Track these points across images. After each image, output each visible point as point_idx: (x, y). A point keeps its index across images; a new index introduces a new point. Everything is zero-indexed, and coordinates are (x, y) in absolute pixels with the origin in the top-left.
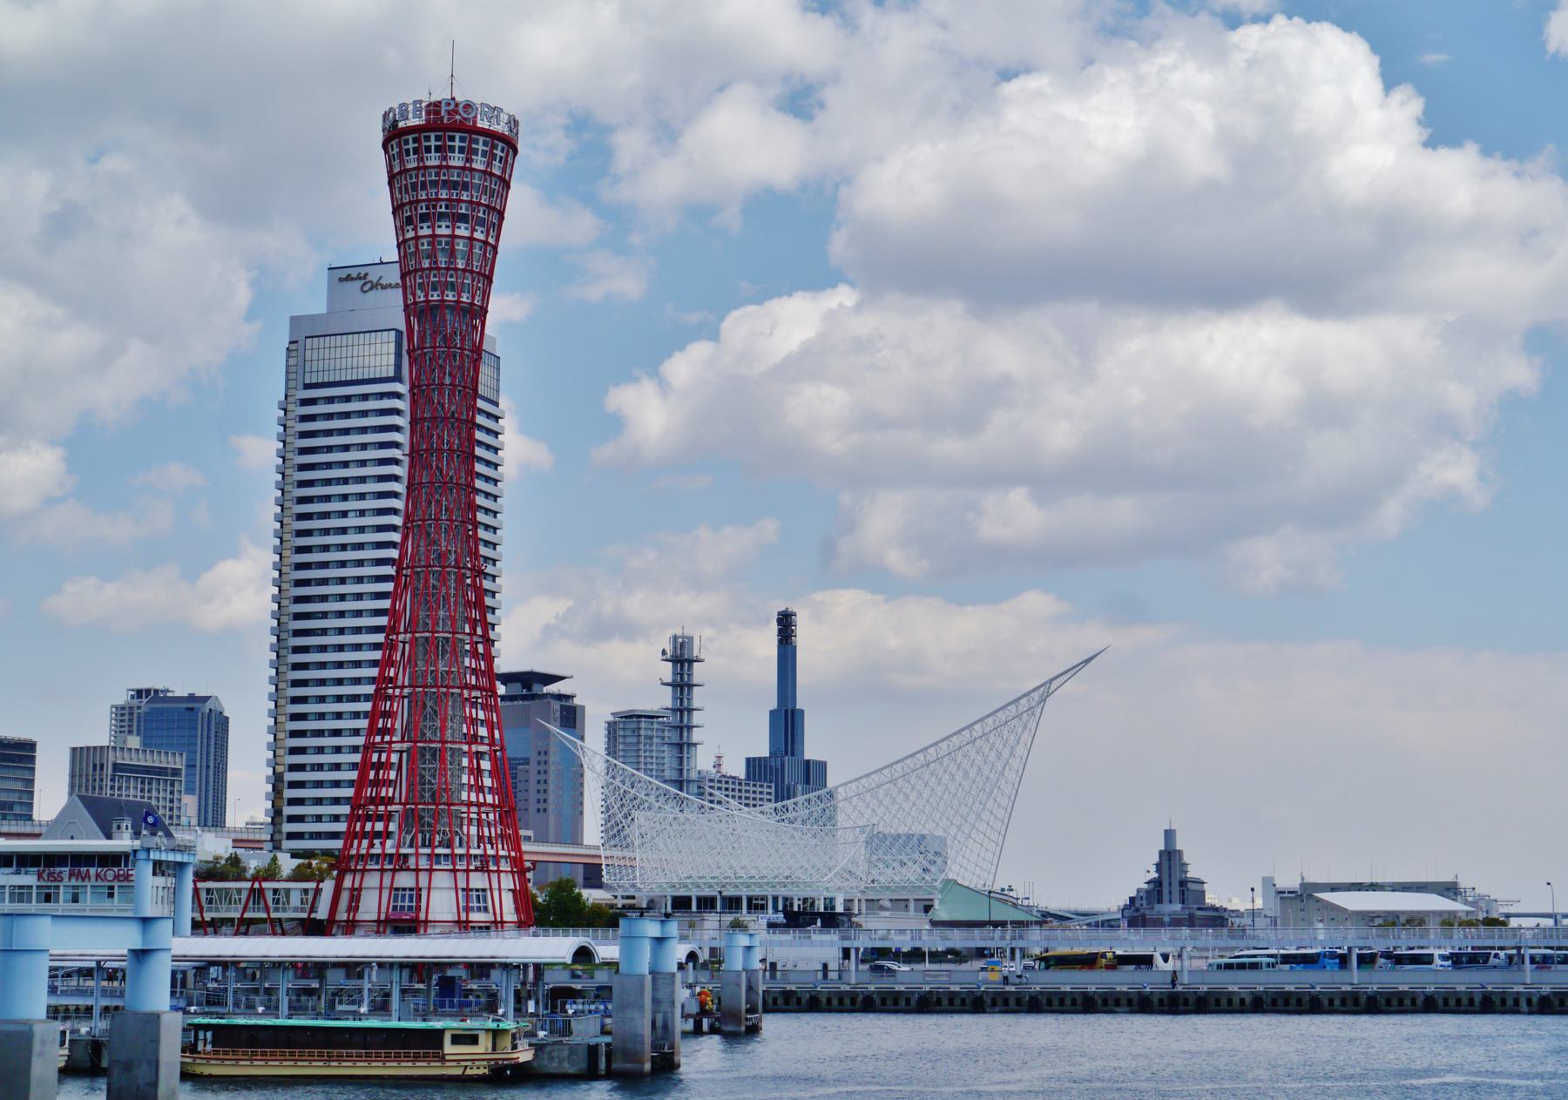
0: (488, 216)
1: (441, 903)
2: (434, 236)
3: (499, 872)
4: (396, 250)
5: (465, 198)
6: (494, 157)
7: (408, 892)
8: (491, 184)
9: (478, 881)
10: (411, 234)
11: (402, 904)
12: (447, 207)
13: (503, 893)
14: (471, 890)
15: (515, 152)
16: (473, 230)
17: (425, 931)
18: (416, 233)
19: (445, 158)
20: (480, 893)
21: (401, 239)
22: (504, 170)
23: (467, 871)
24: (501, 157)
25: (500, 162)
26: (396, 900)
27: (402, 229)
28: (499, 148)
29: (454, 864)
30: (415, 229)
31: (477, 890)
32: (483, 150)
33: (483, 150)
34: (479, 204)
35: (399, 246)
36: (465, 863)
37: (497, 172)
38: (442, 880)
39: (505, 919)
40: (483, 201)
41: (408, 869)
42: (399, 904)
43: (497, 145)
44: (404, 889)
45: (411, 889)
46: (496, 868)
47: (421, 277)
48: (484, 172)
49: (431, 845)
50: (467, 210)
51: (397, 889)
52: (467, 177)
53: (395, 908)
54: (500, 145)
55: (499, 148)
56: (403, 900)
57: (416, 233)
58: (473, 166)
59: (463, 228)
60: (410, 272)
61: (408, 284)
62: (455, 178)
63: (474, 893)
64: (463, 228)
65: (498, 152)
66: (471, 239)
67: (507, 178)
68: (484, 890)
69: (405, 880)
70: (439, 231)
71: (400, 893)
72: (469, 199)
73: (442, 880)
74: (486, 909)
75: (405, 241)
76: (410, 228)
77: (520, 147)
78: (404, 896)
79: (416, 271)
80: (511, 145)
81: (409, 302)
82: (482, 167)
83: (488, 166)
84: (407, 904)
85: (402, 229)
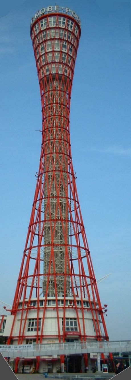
3: (82, 309)
7: (35, 321)
11: (32, 327)
13: (85, 321)
14: (68, 319)
17: (41, 343)
20: (73, 321)
23: (64, 308)
26: (29, 326)
31: (71, 319)
39: (87, 334)
41: (34, 308)
42: (31, 327)
44: (33, 319)
45: (36, 319)
51: (30, 319)
53: (29, 330)
56: (32, 325)
63: (69, 321)
68: (75, 319)
69: (33, 315)
71: (31, 321)
78: (33, 323)
84: (34, 327)
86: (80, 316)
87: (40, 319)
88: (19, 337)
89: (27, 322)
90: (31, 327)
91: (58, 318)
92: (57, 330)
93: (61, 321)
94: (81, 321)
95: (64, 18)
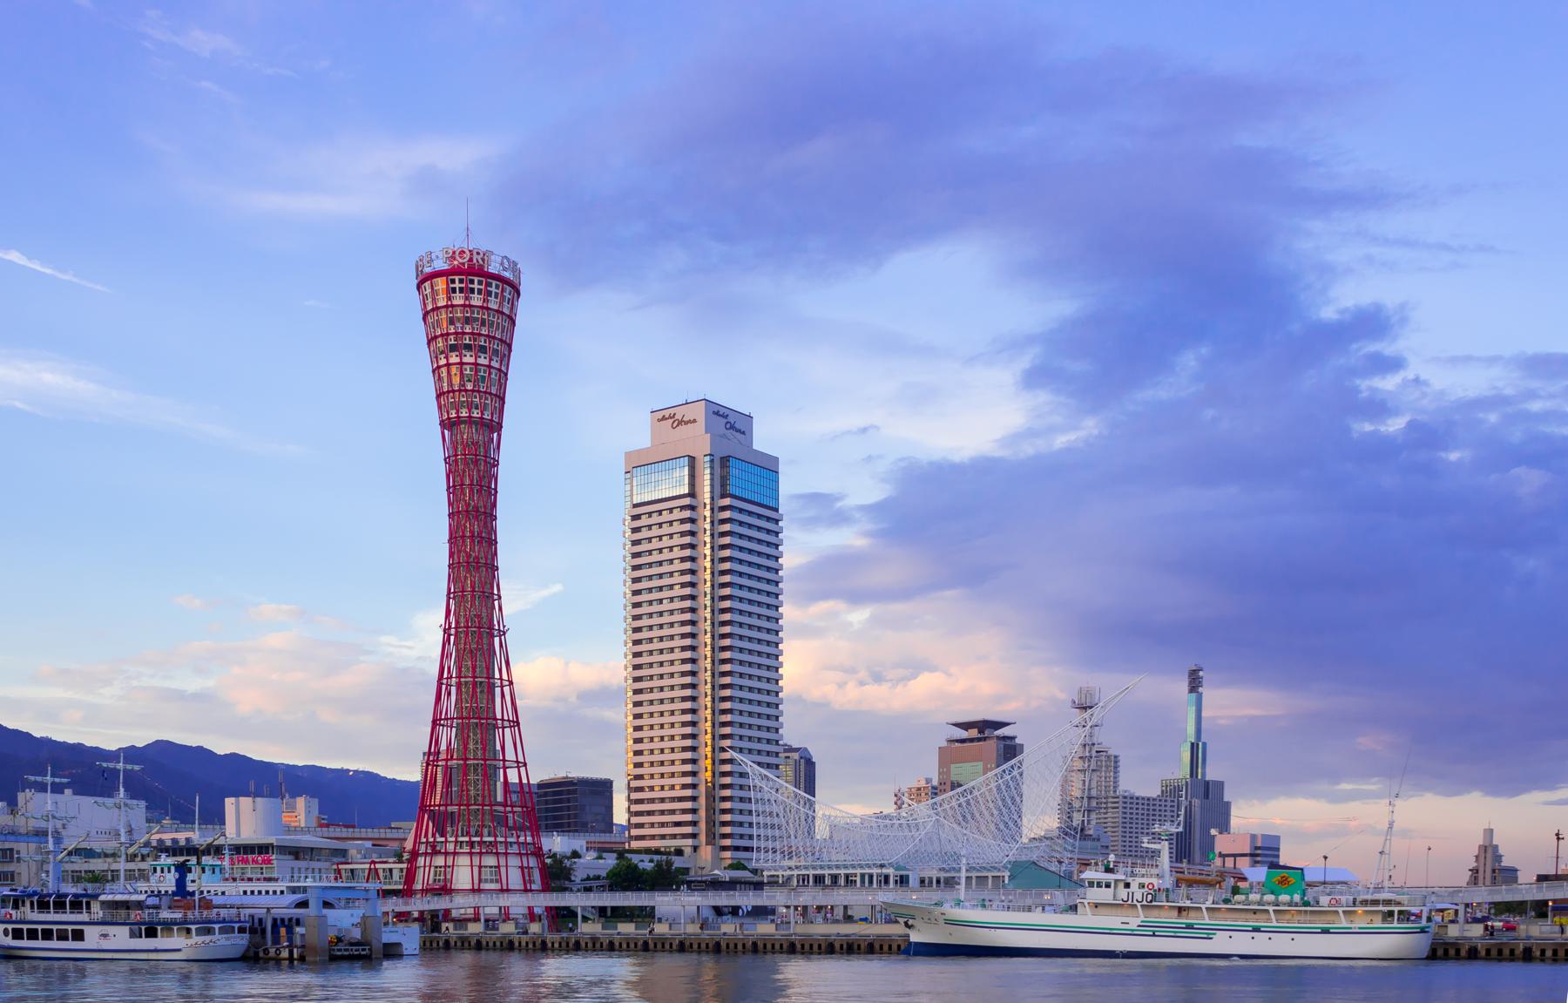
0: (490, 344)
1: (463, 877)
2: (476, 364)
3: (506, 854)
4: (432, 374)
5: (467, 331)
6: (503, 297)
8: (489, 316)
9: (490, 861)
10: (443, 362)
12: (470, 340)
14: (486, 867)
15: (519, 295)
16: (491, 360)
18: (447, 360)
19: (450, 300)
21: (435, 365)
22: (501, 304)
24: (496, 294)
25: (496, 297)
27: (437, 357)
28: (508, 291)
29: (506, 849)
30: (447, 358)
31: (491, 867)
32: (478, 289)
33: (478, 289)
34: (494, 338)
35: (434, 371)
36: (504, 848)
37: (506, 311)
38: (464, 860)
40: (483, 332)
41: (440, 852)
42: (438, 878)
43: (491, 283)
45: (441, 867)
46: (525, 852)
47: (453, 398)
48: (497, 311)
49: (468, 834)
50: (485, 342)
52: (467, 313)
54: (508, 289)
55: (508, 291)
56: (440, 875)
57: (447, 360)
58: (489, 306)
59: (468, 355)
60: (444, 393)
61: (443, 403)
62: (476, 315)
64: (468, 355)
65: (493, 289)
66: (489, 367)
67: (513, 316)
70: (465, 360)
72: (487, 333)
73: (464, 860)
74: (497, 881)
75: (439, 367)
76: (442, 356)
77: (522, 289)
79: (448, 392)
80: (517, 291)
81: (444, 418)
82: (496, 307)
83: (484, 301)
85: (437, 357)
86: (502, 862)
87: (449, 867)
88: (422, 890)
89: (432, 869)
90: (438, 878)
91: (472, 866)
92: (471, 882)
93: (476, 870)
94: (503, 870)
95: (481, 279)
